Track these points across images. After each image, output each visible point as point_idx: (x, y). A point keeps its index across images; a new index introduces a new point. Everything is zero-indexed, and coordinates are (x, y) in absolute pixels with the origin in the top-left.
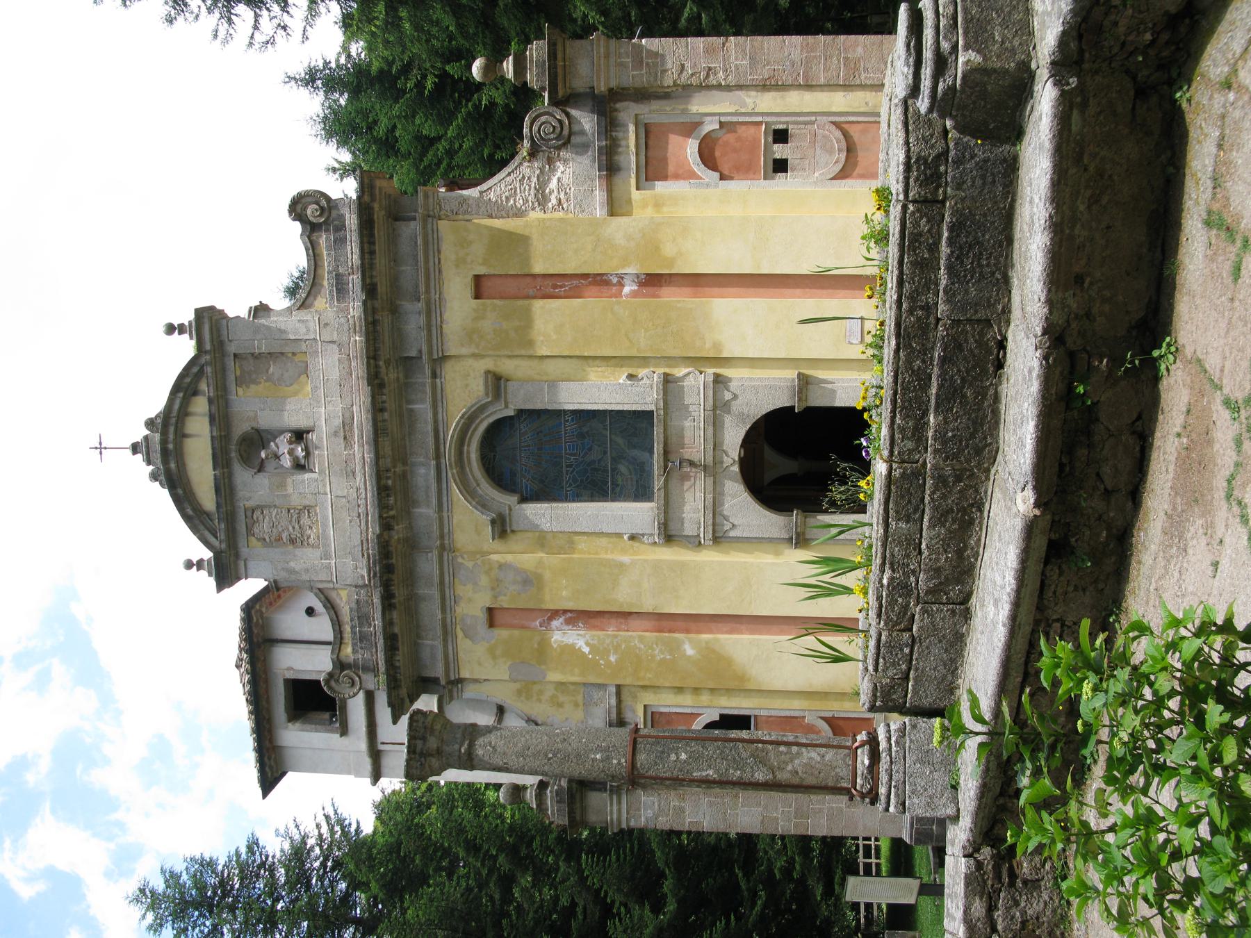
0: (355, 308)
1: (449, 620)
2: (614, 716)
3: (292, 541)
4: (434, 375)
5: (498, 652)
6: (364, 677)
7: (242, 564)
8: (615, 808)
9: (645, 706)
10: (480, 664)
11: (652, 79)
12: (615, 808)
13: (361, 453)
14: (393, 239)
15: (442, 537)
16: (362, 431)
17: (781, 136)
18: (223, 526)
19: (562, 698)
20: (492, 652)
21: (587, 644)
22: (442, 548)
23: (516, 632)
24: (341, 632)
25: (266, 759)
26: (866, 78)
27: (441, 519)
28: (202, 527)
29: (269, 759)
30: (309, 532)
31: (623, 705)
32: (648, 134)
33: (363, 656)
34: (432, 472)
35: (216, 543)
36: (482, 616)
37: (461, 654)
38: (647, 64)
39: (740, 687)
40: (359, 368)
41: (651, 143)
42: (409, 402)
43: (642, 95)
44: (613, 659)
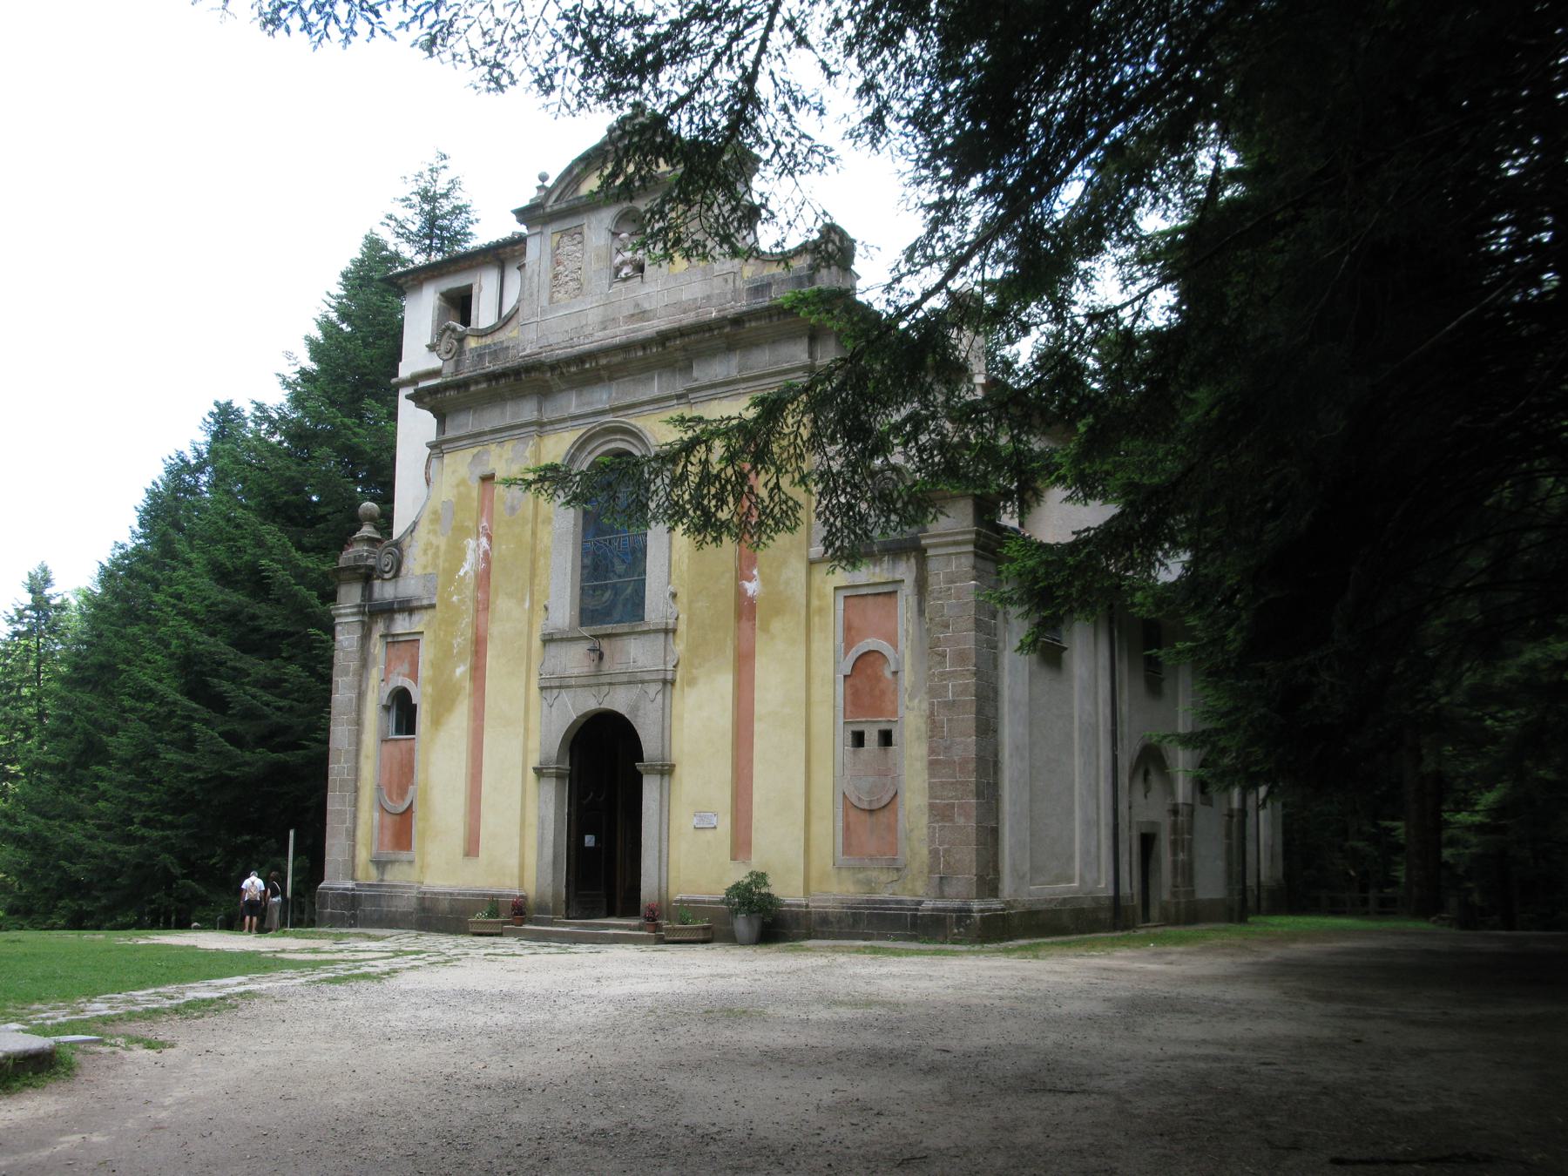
0: (742, 305)
1: (485, 438)
2: (415, 604)
3: (556, 277)
4: (679, 397)
5: (462, 489)
6: (452, 362)
7: (538, 230)
8: (349, 611)
9: (422, 633)
10: (453, 472)
11: (935, 595)
12: (349, 611)
13: (619, 333)
14: (791, 337)
15: (552, 423)
16: (638, 330)
17: (886, 738)
18: (564, 205)
19: (430, 553)
20: (463, 482)
21: (466, 573)
22: (541, 424)
23: (475, 504)
24: (486, 335)
25: (410, 277)
26: (934, 828)
27: (564, 420)
28: (563, 185)
29: (413, 280)
30: (563, 291)
31: (423, 611)
32: (888, 593)
33: (468, 360)
34: (600, 407)
35: (550, 202)
36: (487, 471)
37: (461, 453)
38: (949, 589)
39: (436, 722)
40: (689, 319)
41: (880, 599)
42: (660, 376)
43: (921, 585)
44: (455, 598)
